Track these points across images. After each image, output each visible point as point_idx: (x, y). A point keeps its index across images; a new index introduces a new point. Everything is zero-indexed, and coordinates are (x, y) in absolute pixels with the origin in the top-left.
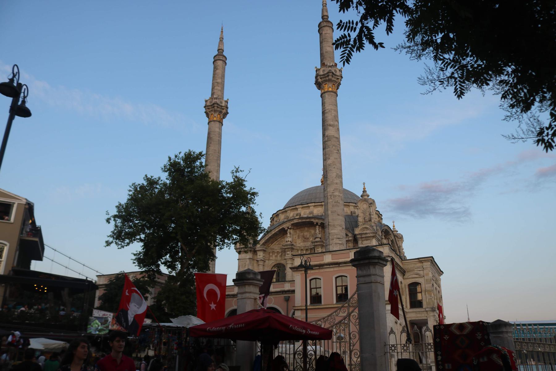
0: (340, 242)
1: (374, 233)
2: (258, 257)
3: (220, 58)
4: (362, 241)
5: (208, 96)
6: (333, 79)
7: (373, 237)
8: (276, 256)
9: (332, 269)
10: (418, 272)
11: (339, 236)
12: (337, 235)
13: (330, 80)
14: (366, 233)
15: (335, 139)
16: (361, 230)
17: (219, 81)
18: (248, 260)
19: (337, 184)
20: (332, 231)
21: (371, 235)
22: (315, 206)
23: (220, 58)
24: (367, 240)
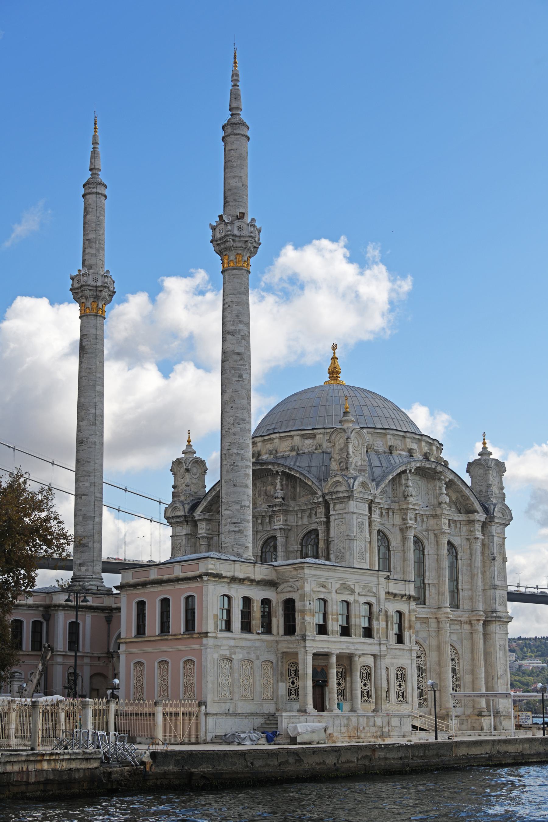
0: (237, 529)
1: (348, 491)
2: (200, 532)
3: (93, 187)
4: (335, 504)
5: (76, 266)
6: (236, 245)
7: (349, 497)
9: (156, 589)
11: (234, 520)
12: (232, 517)
13: (229, 249)
14: (337, 492)
15: (235, 357)
16: (332, 485)
17: (92, 236)
18: (184, 538)
19: (234, 434)
20: (225, 512)
21: (345, 495)
22: (281, 438)
23: (93, 187)
24: (341, 503)
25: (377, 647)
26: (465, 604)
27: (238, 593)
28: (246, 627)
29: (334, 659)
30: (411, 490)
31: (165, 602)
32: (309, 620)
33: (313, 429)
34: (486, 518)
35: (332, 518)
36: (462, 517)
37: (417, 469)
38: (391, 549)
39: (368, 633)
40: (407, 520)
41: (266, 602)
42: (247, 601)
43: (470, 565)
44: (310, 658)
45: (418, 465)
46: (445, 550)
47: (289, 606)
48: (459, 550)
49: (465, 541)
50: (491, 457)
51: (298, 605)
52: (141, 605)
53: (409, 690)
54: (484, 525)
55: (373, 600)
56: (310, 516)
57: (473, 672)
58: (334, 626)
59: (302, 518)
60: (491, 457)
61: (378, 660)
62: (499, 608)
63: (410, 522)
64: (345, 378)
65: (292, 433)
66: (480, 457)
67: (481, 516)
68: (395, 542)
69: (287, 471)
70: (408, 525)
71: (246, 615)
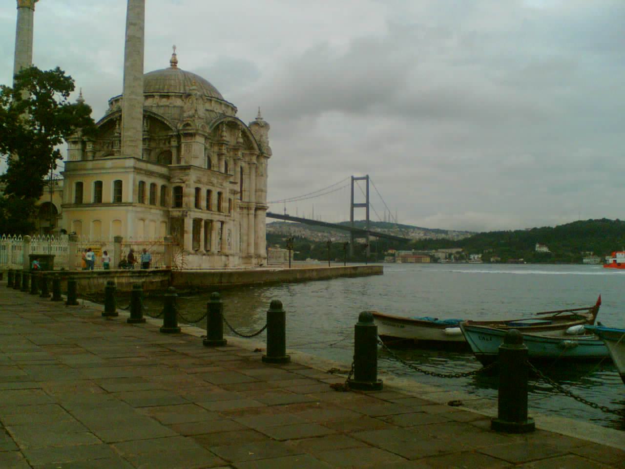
2: (87, 148)
8: (108, 147)
10: (182, 178)
25: (224, 217)
26: (245, 199)
27: (149, 181)
28: (153, 201)
29: (203, 223)
30: (225, 134)
31: (99, 185)
32: (189, 199)
33: (168, 93)
34: (259, 153)
35: (183, 145)
36: (247, 152)
37: (229, 122)
38: (212, 165)
39: (219, 210)
40: (222, 149)
41: (164, 188)
42: (153, 186)
43: (250, 178)
44: (191, 222)
45: (230, 119)
46: (239, 169)
47: (179, 191)
48: (244, 169)
49: (247, 165)
50: (262, 120)
51: (186, 190)
52: (80, 185)
53: (232, 242)
54: (258, 157)
55: (223, 191)
56: (165, 144)
57: (248, 235)
58: (203, 203)
59: (159, 143)
60: (262, 120)
61: (224, 226)
62: (264, 202)
63: (224, 151)
64: (179, 66)
65: (154, 94)
66: (255, 120)
67: (257, 152)
68: (215, 160)
69: (152, 115)
70: (223, 153)
71: (153, 193)
